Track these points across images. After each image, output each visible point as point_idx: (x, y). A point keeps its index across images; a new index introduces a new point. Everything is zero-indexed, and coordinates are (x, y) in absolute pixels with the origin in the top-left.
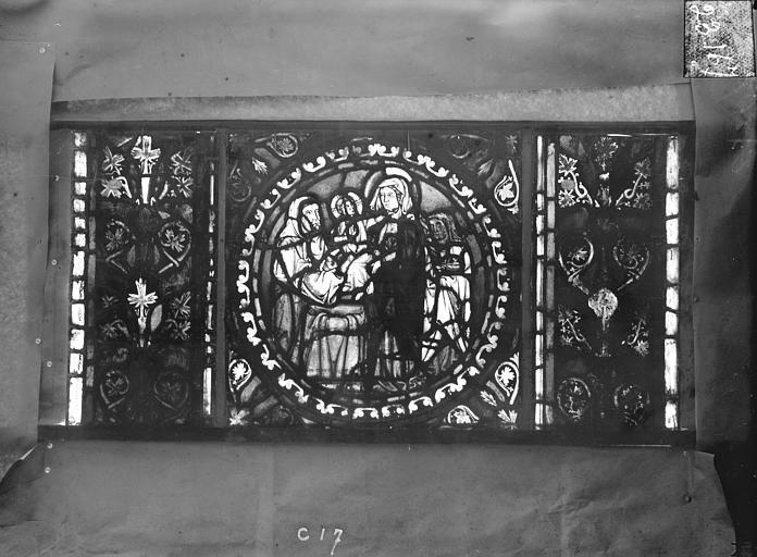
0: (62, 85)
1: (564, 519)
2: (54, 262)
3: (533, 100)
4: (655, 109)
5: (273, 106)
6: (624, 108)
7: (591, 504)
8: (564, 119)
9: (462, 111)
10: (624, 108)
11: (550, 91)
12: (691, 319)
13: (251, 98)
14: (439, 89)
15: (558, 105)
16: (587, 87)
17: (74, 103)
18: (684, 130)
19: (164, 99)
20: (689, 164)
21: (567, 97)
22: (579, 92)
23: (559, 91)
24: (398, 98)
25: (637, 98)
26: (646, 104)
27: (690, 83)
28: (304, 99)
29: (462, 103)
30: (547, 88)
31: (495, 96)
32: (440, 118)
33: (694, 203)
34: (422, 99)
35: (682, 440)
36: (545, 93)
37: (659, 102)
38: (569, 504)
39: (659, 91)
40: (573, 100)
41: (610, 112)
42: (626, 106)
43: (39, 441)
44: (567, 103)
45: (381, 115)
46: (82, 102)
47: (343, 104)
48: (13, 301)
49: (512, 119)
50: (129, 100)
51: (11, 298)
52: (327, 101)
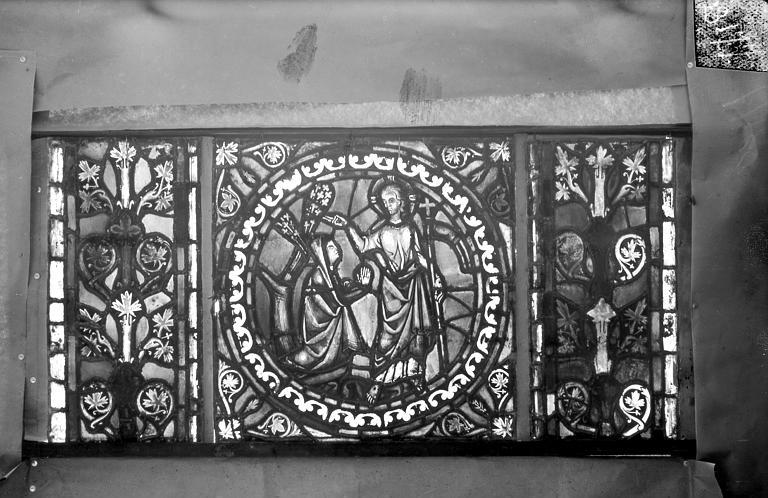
0: (43, 94)
2: (37, 276)
3: (526, 104)
4: (650, 113)
5: (260, 114)
6: (619, 112)
8: (555, 124)
9: (453, 116)
10: (619, 112)
13: (236, 106)
15: (551, 110)
17: (57, 115)
18: (682, 132)
19: (148, 108)
21: (560, 100)
22: (572, 95)
23: (552, 96)
24: (388, 104)
25: (632, 101)
26: (641, 107)
27: (687, 85)
29: (454, 108)
31: (486, 101)
33: (690, 207)
35: (683, 448)
36: (538, 96)
37: (655, 105)
39: (655, 93)
40: (566, 104)
41: (604, 116)
42: (620, 110)
43: (23, 459)
44: (561, 107)
46: (64, 112)
47: (331, 111)
49: (505, 124)
50: (112, 109)
52: (315, 107)
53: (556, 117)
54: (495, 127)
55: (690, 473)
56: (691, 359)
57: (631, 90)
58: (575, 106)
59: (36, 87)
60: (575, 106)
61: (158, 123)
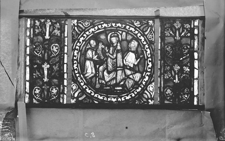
0: (22, 5)
1: (167, 130)
4: (193, 13)
5: (84, 11)
7: (175, 126)
9: (138, 13)
10: (185, 12)
11: (163, 7)
12: (204, 73)
13: (77, 9)
14: (132, 7)
16: (174, 6)
17: (26, 11)
18: (202, 18)
19: (52, 9)
20: (203, 29)
21: (168, 9)
22: (172, 8)
23: (166, 7)
24: (120, 9)
28: (92, 10)
30: (163, 7)
32: (132, 15)
34: (126, 9)
35: (201, 108)
36: (162, 8)
37: (195, 11)
38: (168, 126)
39: (195, 7)
41: (181, 13)
45: (115, 14)
46: (28, 10)
47: (104, 11)
48: (8, 67)
50: (42, 10)
51: (7, 67)
53: (167, 14)
54: (149, 16)
55: (203, 115)
56: (204, 82)
57: (188, 7)
58: (172, 11)
59: (20, 3)
60: (172, 11)
61: (55, 13)
